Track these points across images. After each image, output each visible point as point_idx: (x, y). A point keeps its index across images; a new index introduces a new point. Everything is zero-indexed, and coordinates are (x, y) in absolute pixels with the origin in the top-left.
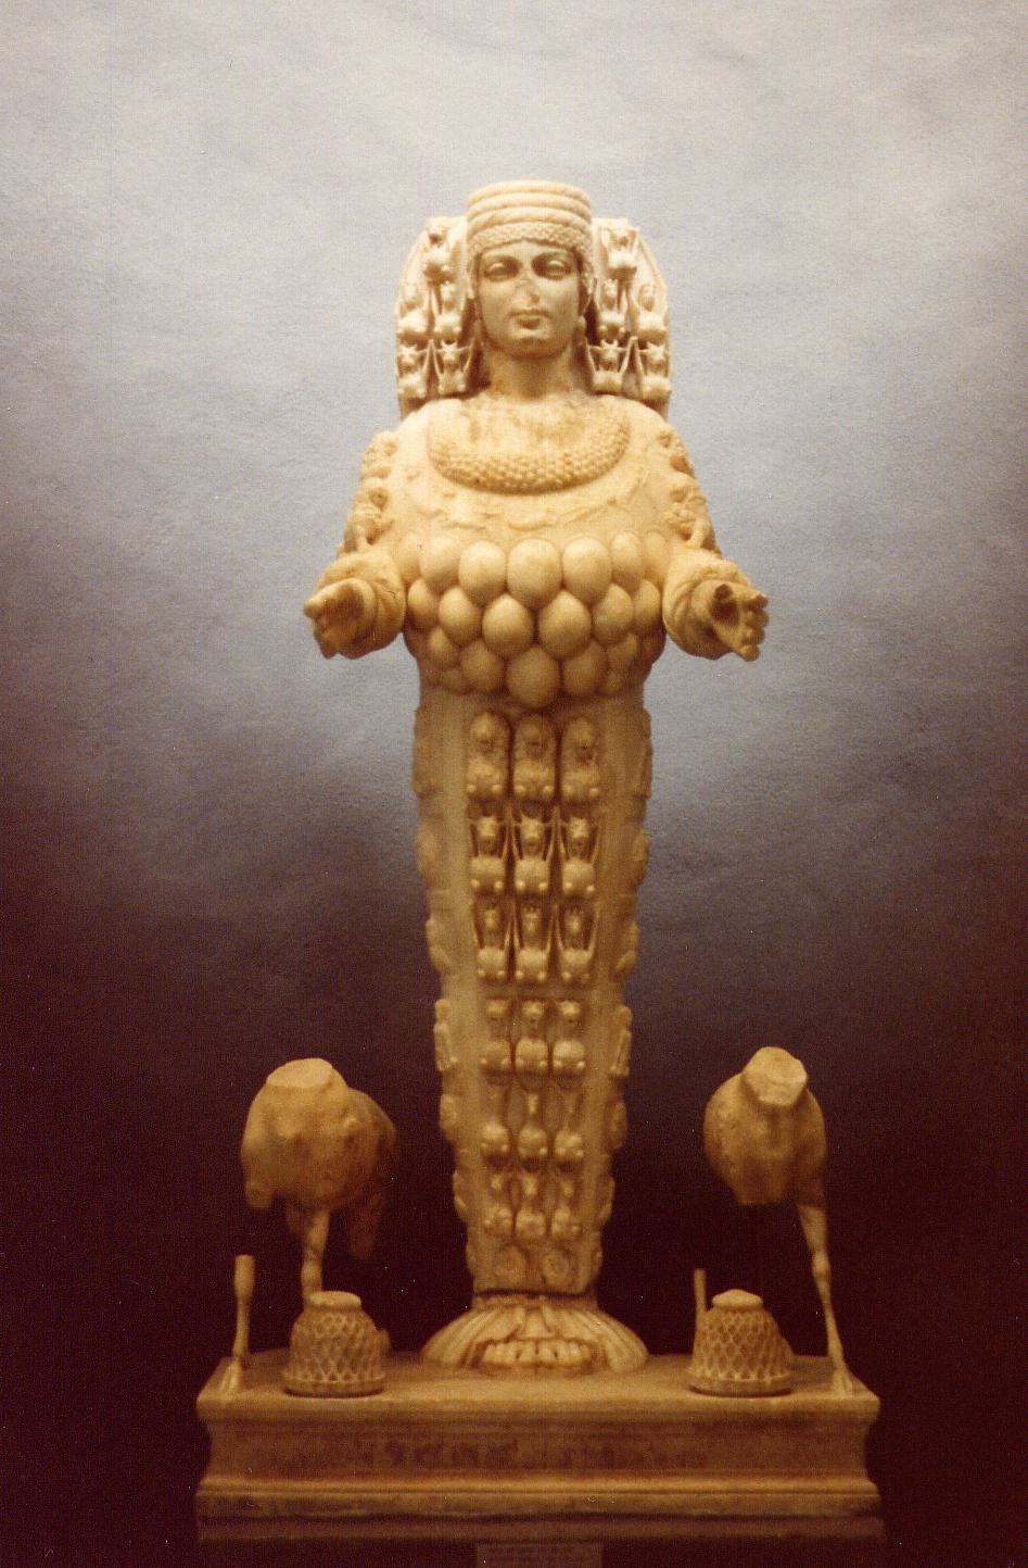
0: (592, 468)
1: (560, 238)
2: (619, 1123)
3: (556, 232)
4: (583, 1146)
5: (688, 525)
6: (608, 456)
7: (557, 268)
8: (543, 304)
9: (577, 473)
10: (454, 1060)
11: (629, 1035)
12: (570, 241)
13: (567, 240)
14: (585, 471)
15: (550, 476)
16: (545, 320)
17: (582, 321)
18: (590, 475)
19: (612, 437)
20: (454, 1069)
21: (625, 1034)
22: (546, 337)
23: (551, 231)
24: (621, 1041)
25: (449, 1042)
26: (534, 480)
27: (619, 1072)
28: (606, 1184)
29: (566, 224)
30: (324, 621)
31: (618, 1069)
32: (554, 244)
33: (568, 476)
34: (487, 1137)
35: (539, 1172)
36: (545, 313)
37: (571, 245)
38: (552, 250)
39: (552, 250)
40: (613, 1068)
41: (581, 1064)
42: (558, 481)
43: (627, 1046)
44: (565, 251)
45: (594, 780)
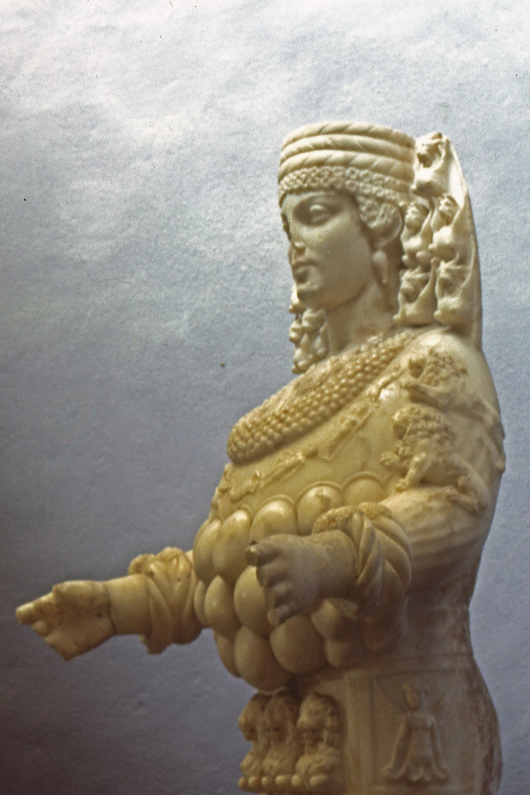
0: (303, 420)
1: (314, 181)
3: (308, 175)
5: (405, 463)
6: (327, 404)
7: (318, 212)
8: (309, 254)
9: (286, 429)
12: (326, 181)
13: (322, 180)
14: (294, 425)
15: (263, 438)
16: (312, 269)
17: (380, 256)
18: (301, 429)
19: (343, 381)
22: (316, 287)
23: (303, 176)
26: (252, 446)
29: (320, 163)
30: (39, 625)
32: (310, 189)
33: (277, 435)
36: (311, 262)
37: (326, 185)
38: (305, 196)
39: (305, 196)
42: (269, 443)
44: (322, 193)
45: (315, 766)
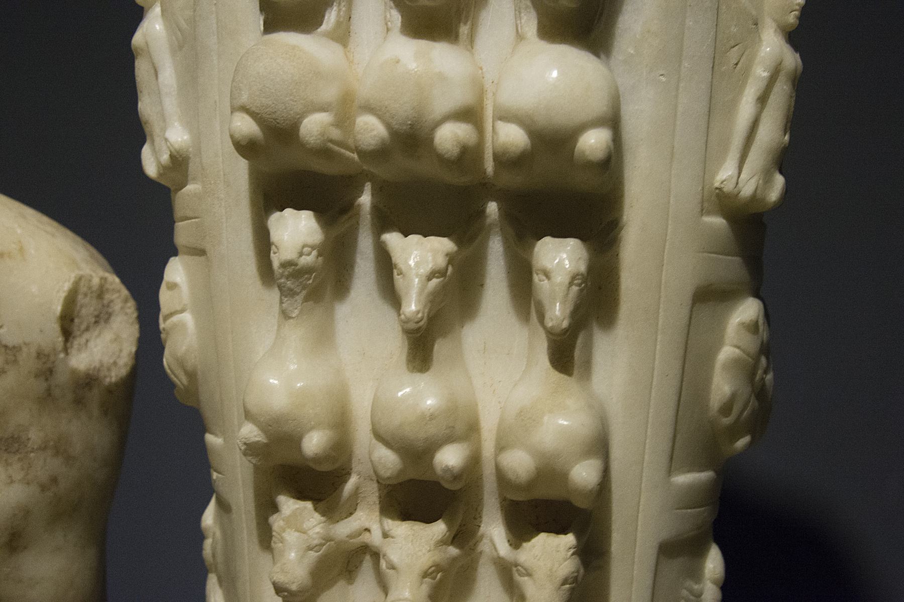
2: (747, 370)
4: (600, 446)
10: (177, 135)
11: (791, 60)
20: (179, 163)
21: (771, 49)
24: (761, 72)
25: (168, 76)
27: (747, 189)
28: (696, 574)
31: (747, 175)
34: (254, 401)
35: (439, 528)
40: (725, 175)
41: (593, 142)
43: (781, 93)
